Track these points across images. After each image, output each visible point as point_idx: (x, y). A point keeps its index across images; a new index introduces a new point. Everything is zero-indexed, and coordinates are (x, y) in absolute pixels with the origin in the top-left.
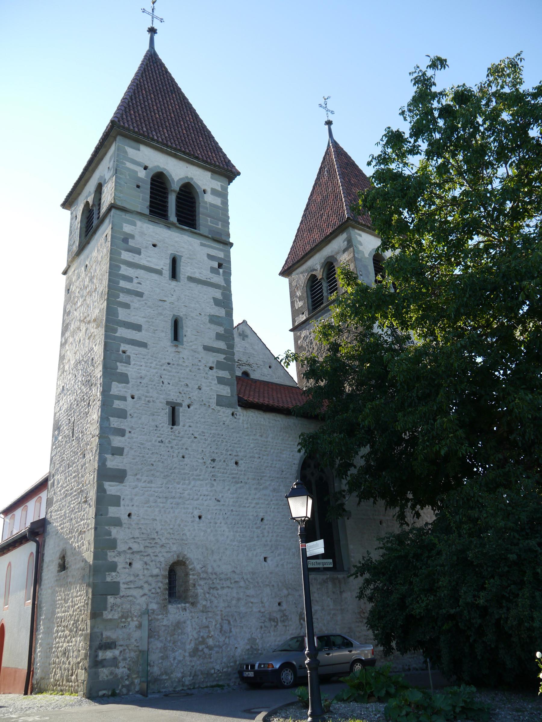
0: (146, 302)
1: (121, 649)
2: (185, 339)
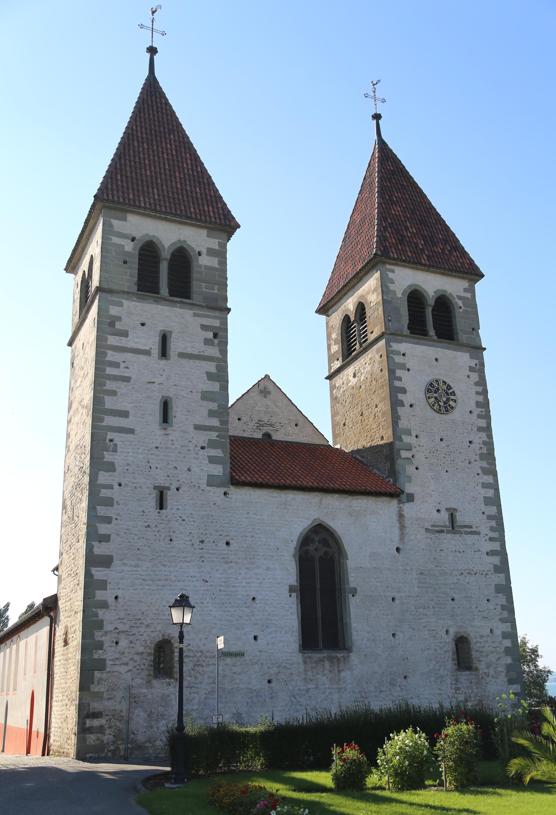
0: (133, 386)
1: (108, 718)
2: (175, 420)
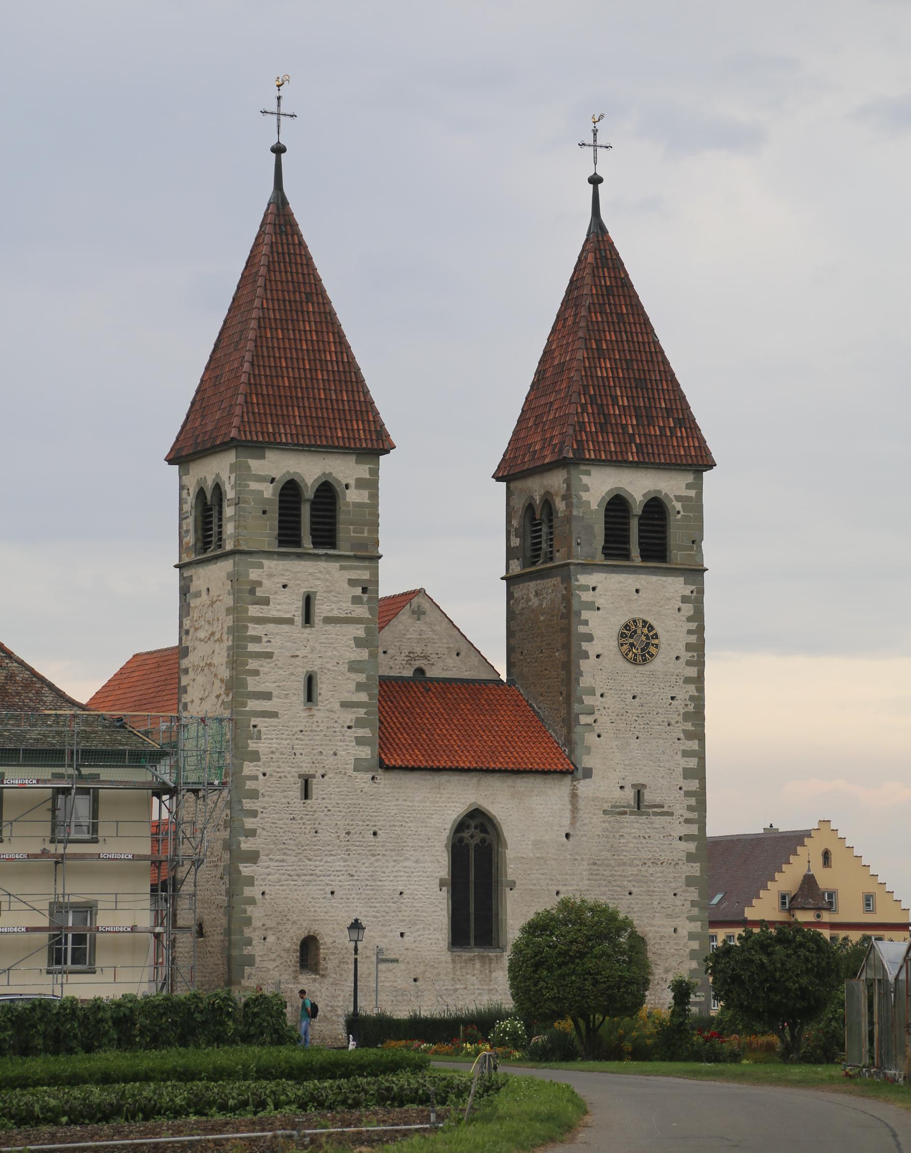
2: (320, 698)
